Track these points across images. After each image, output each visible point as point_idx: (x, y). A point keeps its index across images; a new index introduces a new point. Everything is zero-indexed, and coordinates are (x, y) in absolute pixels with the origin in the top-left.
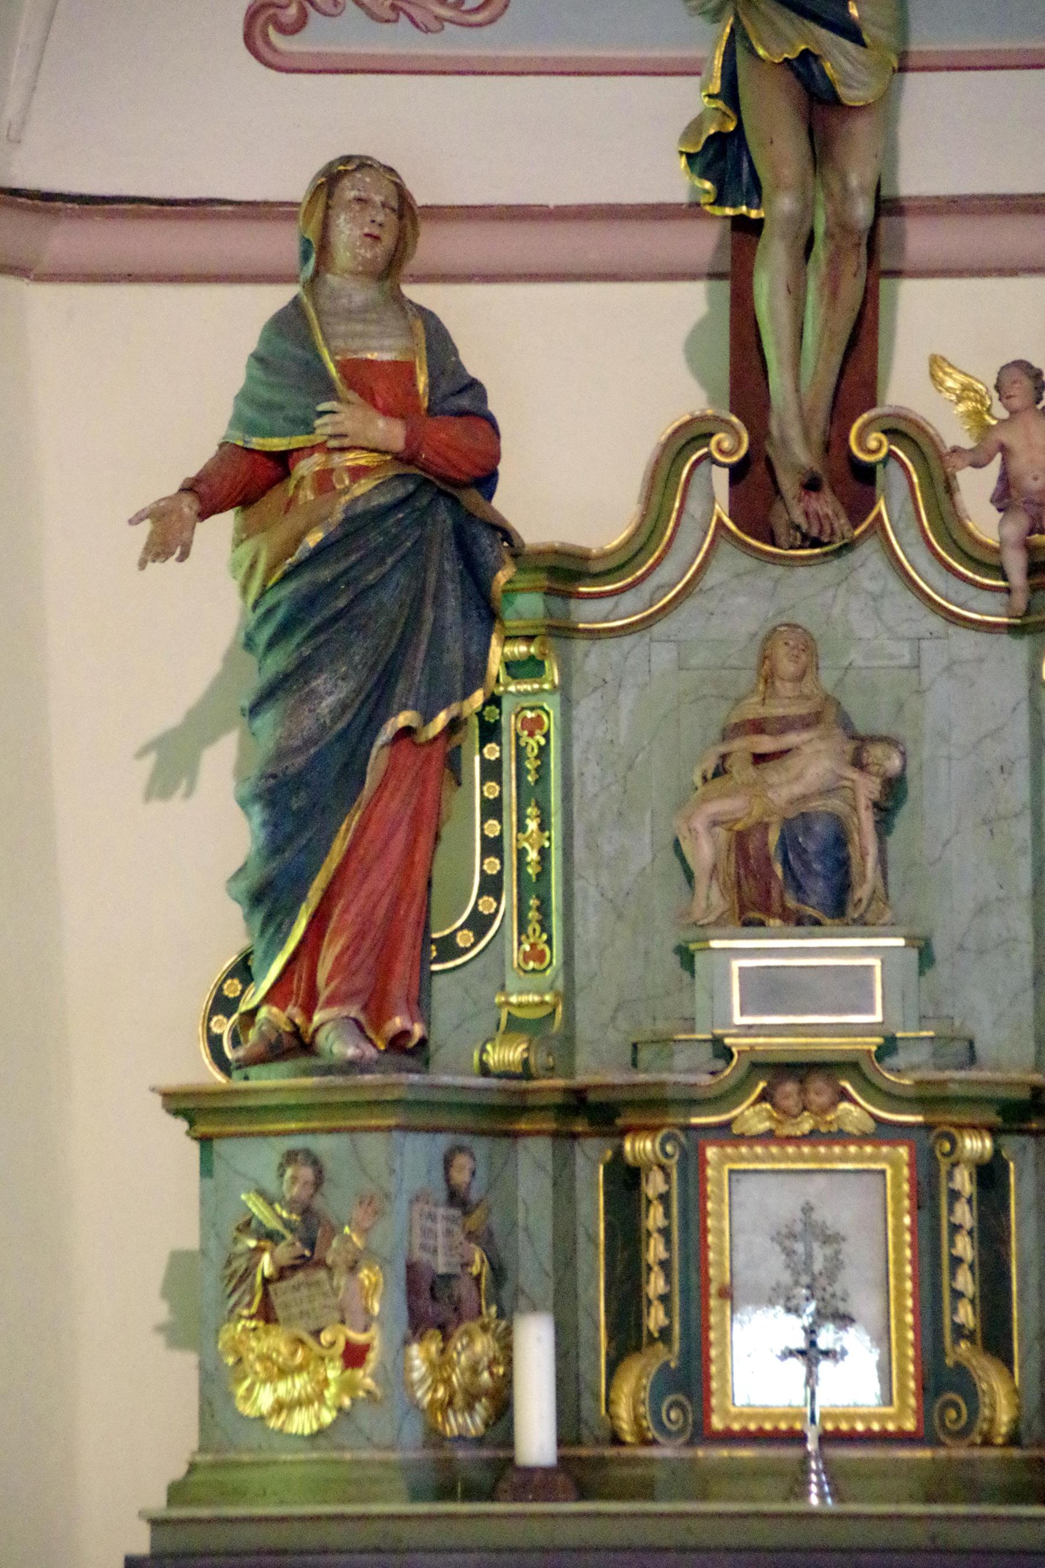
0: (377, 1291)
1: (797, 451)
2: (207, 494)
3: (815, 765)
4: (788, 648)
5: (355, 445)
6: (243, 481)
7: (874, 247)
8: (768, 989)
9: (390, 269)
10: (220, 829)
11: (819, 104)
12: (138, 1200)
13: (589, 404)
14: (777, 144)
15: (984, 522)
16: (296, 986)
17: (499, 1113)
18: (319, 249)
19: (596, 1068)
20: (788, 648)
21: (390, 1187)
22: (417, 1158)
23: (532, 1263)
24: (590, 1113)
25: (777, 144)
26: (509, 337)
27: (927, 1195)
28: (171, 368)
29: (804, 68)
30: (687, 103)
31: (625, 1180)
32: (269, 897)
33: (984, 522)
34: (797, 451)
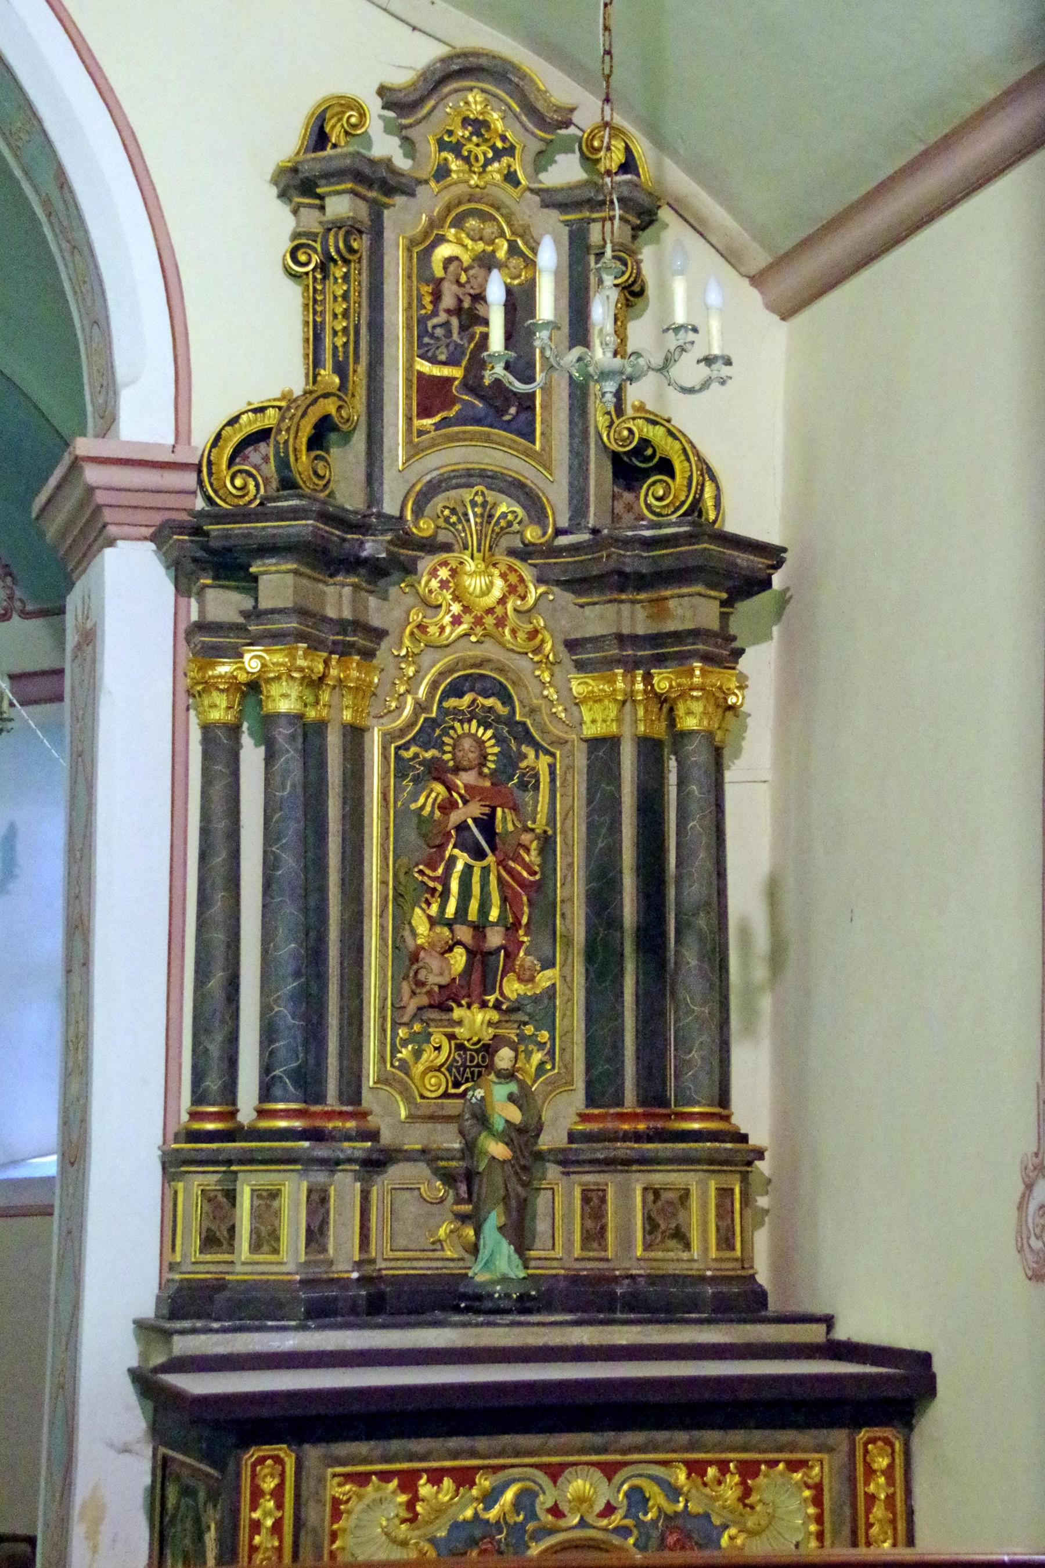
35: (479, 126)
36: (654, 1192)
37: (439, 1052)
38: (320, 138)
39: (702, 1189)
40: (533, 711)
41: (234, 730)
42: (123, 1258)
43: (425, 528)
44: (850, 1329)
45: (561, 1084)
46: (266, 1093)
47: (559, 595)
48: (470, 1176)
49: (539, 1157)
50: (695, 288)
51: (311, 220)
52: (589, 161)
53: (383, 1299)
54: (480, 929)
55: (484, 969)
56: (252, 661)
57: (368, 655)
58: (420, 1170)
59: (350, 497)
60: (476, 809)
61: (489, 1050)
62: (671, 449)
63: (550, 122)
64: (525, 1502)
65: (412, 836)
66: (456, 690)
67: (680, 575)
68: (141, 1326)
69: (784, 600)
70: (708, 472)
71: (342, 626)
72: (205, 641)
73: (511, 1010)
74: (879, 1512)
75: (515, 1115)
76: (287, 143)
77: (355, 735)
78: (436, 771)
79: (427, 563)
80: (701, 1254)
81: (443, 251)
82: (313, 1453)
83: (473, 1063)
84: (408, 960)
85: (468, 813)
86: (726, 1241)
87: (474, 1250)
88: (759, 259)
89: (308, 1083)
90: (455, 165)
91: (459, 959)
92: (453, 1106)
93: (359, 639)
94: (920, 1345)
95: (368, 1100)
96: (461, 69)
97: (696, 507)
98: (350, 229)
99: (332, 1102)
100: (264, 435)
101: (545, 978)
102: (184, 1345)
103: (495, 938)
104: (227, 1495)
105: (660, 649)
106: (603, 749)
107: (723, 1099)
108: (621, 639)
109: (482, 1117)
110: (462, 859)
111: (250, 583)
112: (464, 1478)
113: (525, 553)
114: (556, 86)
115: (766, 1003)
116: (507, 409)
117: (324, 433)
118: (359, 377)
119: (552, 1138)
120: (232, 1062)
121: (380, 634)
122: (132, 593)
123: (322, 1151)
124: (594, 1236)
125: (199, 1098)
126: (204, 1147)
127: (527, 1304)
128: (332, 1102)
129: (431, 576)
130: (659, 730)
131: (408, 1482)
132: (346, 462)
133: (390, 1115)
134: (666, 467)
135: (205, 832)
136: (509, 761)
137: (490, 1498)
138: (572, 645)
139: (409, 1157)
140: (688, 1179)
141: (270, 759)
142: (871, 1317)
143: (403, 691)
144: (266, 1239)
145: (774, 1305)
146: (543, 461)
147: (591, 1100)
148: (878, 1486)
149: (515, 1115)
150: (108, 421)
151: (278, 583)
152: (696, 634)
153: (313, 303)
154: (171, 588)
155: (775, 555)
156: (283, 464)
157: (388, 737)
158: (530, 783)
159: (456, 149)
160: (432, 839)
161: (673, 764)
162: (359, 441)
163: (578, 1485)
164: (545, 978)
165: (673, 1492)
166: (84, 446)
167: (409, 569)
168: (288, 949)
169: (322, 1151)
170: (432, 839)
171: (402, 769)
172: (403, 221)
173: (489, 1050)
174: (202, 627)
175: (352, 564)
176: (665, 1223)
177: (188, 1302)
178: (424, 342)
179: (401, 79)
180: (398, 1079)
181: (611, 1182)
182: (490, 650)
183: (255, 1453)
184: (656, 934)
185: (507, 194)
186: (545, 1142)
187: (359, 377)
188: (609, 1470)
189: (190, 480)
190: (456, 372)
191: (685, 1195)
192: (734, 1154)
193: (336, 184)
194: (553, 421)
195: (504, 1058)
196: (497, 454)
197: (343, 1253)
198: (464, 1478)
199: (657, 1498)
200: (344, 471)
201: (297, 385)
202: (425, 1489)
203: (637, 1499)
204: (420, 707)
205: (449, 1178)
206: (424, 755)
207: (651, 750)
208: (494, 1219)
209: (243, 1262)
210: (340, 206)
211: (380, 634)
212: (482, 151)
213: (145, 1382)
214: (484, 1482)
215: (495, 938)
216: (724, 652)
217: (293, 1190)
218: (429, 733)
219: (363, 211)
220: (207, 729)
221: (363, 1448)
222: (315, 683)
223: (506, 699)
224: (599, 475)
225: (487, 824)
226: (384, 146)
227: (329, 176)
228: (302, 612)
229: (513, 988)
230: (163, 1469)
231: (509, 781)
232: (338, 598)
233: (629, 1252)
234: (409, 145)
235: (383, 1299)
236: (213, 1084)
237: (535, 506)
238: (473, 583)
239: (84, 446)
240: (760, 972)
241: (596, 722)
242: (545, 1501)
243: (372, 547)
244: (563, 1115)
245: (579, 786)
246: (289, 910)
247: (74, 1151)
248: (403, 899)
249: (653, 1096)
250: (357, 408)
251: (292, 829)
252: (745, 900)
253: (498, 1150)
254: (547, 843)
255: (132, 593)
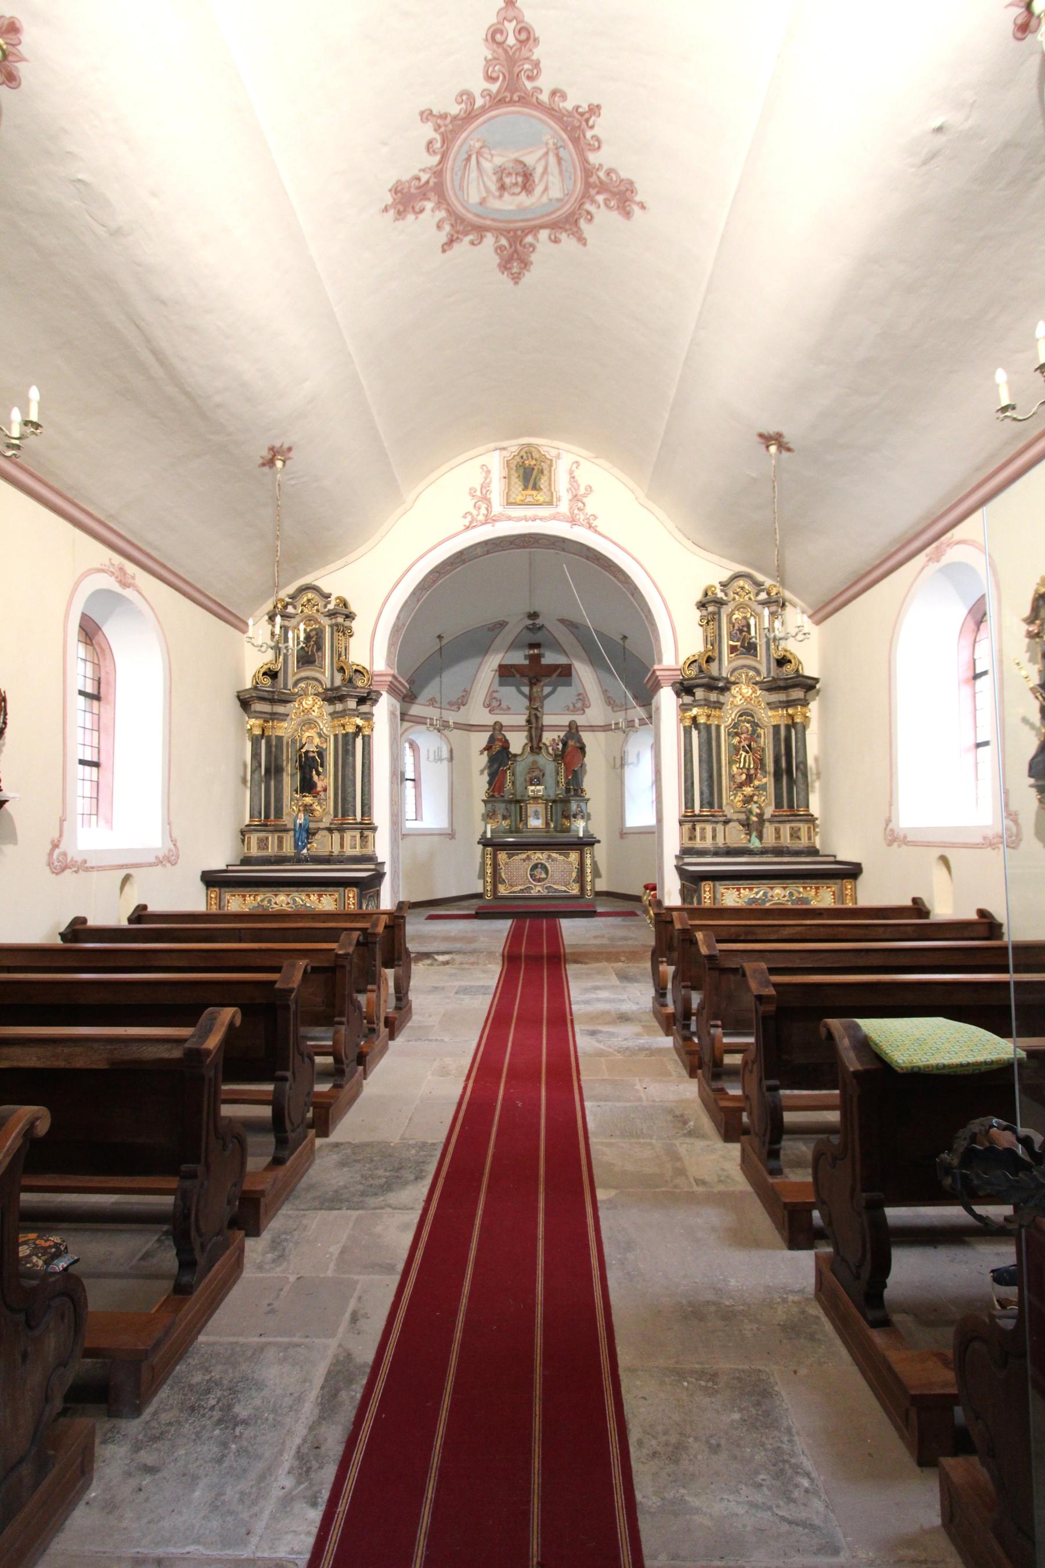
0: (500, 817)
1: (535, 745)
2: (485, 749)
3: (536, 773)
4: (534, 762)
5: (497, 746)
6: (488, 748)
7: (541, 729)
8: (533, 791)
9: (501, 730)
10: (486, 778)
11: (537, 717)
12: (480, 809)
13: (517, 742)
14: (533, 720)
15: (551, 751)
16: (493, 791)
17: (510, 802)
18: (494, 729)
19: (519, 798)
20: (534, 762)
21: (501, 807)
22: (503, 805)
23: (513, 814)
24: (518, 802)
25: (533, 720)
26: (510, 736)
27: (546, 809)
28: (481, 739)
29: (535, 715)
30: (526, 717)
31: (521, 807)
32: (490, 783)
33: (551, 751)
34: (535, 745)
35: (742, 588)
36: (792, 828)
37: (740, 797)
38: (706, 594)
39: (804, 827)
40: (759, 719)
41: (690, 727)
42: (672, 843)
43: (733, 679)
44: (840, 857)
45: (769, 804)
46: (702, 806)
47: (764, 693)
48: (748, 825)
49: (764, 821)
50: (796, 618)
51: (705, 613)
52: (768, 594)
53: (730, 852)
54: (748, 769)
55: (750, 779)
56: (695, 711)
57: (720, 708)
58: (736, 824)
59: (715, 673)
60: (747, 742)
61: (752, 797)
62: (789, 657)
63: (758, 584)
64: (765, 894)
65: (732, 749)
66: (741, 716)
67: (794, 686)
68: (677, 857)
69: (818, 691)
70: (800, 663)
71: (715, 702)
72: (684, 708)
73: (757, 788)
74: (848, 897)
75: (758, 811)
76: (699, 596)
77: (718, 727)
78: (737, 734)
79: (733, 687)
80: (804, 842)
81: (735, 617)
82: (717, 883)
83: (748, 800)
84: (732, 777)
85: (745, 743)
86: (809, 838)
87: (749, 841)
88: (810, 612)
89: (711, 805)
90: (737, 597)
91: (744, 777)
92: (743, 810)
93: (719, 705)
94: (858, 861)
95: (724, 808)
96: (737, 576)
97: (797, 670)
98: (714, 613)
99: (716, 809)
100: (695, 661)
101: (764, 780)
102: (687, 860)
103: (752, 772)
104: (698, 891)
105: (788, 704)
106: (776, 728)
107: (808, 807)
108: (780, 702)
109: (750, 812)
110: (744, 754)
111: (693, 695)
112: (751, 889)
113: (756, 683)
114: (760, 577)
115: (817, 784)
116: (750, 649)
117: (709, 660)
118: (716, 646)
119: (767, 816)
120: (693, 800)
121: (723, 704)
122: (667, 699)
123: (714, 819)
124: (778, 838)
125: (686, 808)
126: (689, 820)
127: (763, 852)
128: (716, 809)
129: (734, 690)
130: (790, 722)
131: (738, 889)
132: (714, 666)
133: (729, 812)
134: (790, 661)
135: (685, 750)
136: (754, 731)
137: (757, 893)
138: (768, 704)
139: (734, 821)
140: (801, 825)
141: (699, 733)
142: (846, 854)
143: (728, 717)
144: (703, 838)
145: (821, 853)
146: (759, 662)
147: (777, 807)
148: (848, 892)
149: (758, 811)
150: (660, 661)
151: (700, 693)
152: (799, 700)
153: (705, 631)
154: (675, 697)
155: (817, 680)
156: (700, 667)
157: (726, 727)
158: (759, 736)
159: (737, 593)
160: (736, 749)
161: (793, 731)
162: (717, 661)
163: (777, 891)
164: (764, 780)
165: (800, 893)
166: (656, 667)
167: (729, 689)
168: (705, 775)
169: (714, 819)
170: (736, 749)
171: (729, 734)
172: (725, 611)
173: (752, 797)
174: (683, 704)
175: (717, 688)
176: (795, 835)
177: (686, 852)
178: (731, 637)
179: (724, 579)
180: (731, 802)
181: (781, 826)
182: (749, 706)
183: (703, 884)
184: (789, 770)
185: (750, 603)
186: (766, 817)
187: (716, 646)
188: (784, 888)
189: (679, 673)
190: (739, 644)
191: (799, 829)
192: (810, 819)
193: (710, 605)
194: (761, 651)
195: (755, 798)
196: (749, 661)
197: (720, 841)
198: (751, 889)
199: (796, 894)
200: (714, 669)
201: (702, 649)
202: (742, 891)
203: (791, 894)
204: (733, 720)
205: (743, 826)
206: (735, 731)
207: (788, 728)
208: (754, 834)
209: (698, 844)
210: (711, 609)
211: (723, 704)
212: (743, 594)
213: (677, 868)
214: (755, 890)
215: (752, 772)
216: (805, 703)
217: (709, 828)
218: (735, 726)
219: (716, 609)
220: (685, 727)
221: (727, 882)
222: (708, 716)
223: (753, 717)
224: (773, 664)
225: (749, 746)
226: (720, 595)
227: (709, 602)
228: (705, 700)
229: (757, 783)
230: (683, 886)
231: (754, 736)
232: (713, 696)
233: (786, 841)
234: (726, 595)
235: (730, 852)
236: (689, 805)
237: (758, 672)
238: (744, 691)
239: (656, 667)
240: (814, 777)
241: (774, 722)
242: (770, 894)
243: (721, 684)
244: (769, 811)
245: (771, 737)
246: (705, 766)
247: (660, 819)
248: (731, 763)
249: (791, 806)
250: (716, 654)
251: (704, 749)
252: (810, 762)
253: (755, 819)
254: (763, 750)
255: (667, 699)
